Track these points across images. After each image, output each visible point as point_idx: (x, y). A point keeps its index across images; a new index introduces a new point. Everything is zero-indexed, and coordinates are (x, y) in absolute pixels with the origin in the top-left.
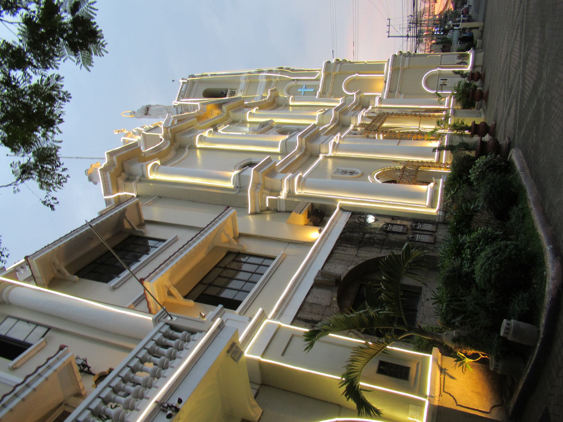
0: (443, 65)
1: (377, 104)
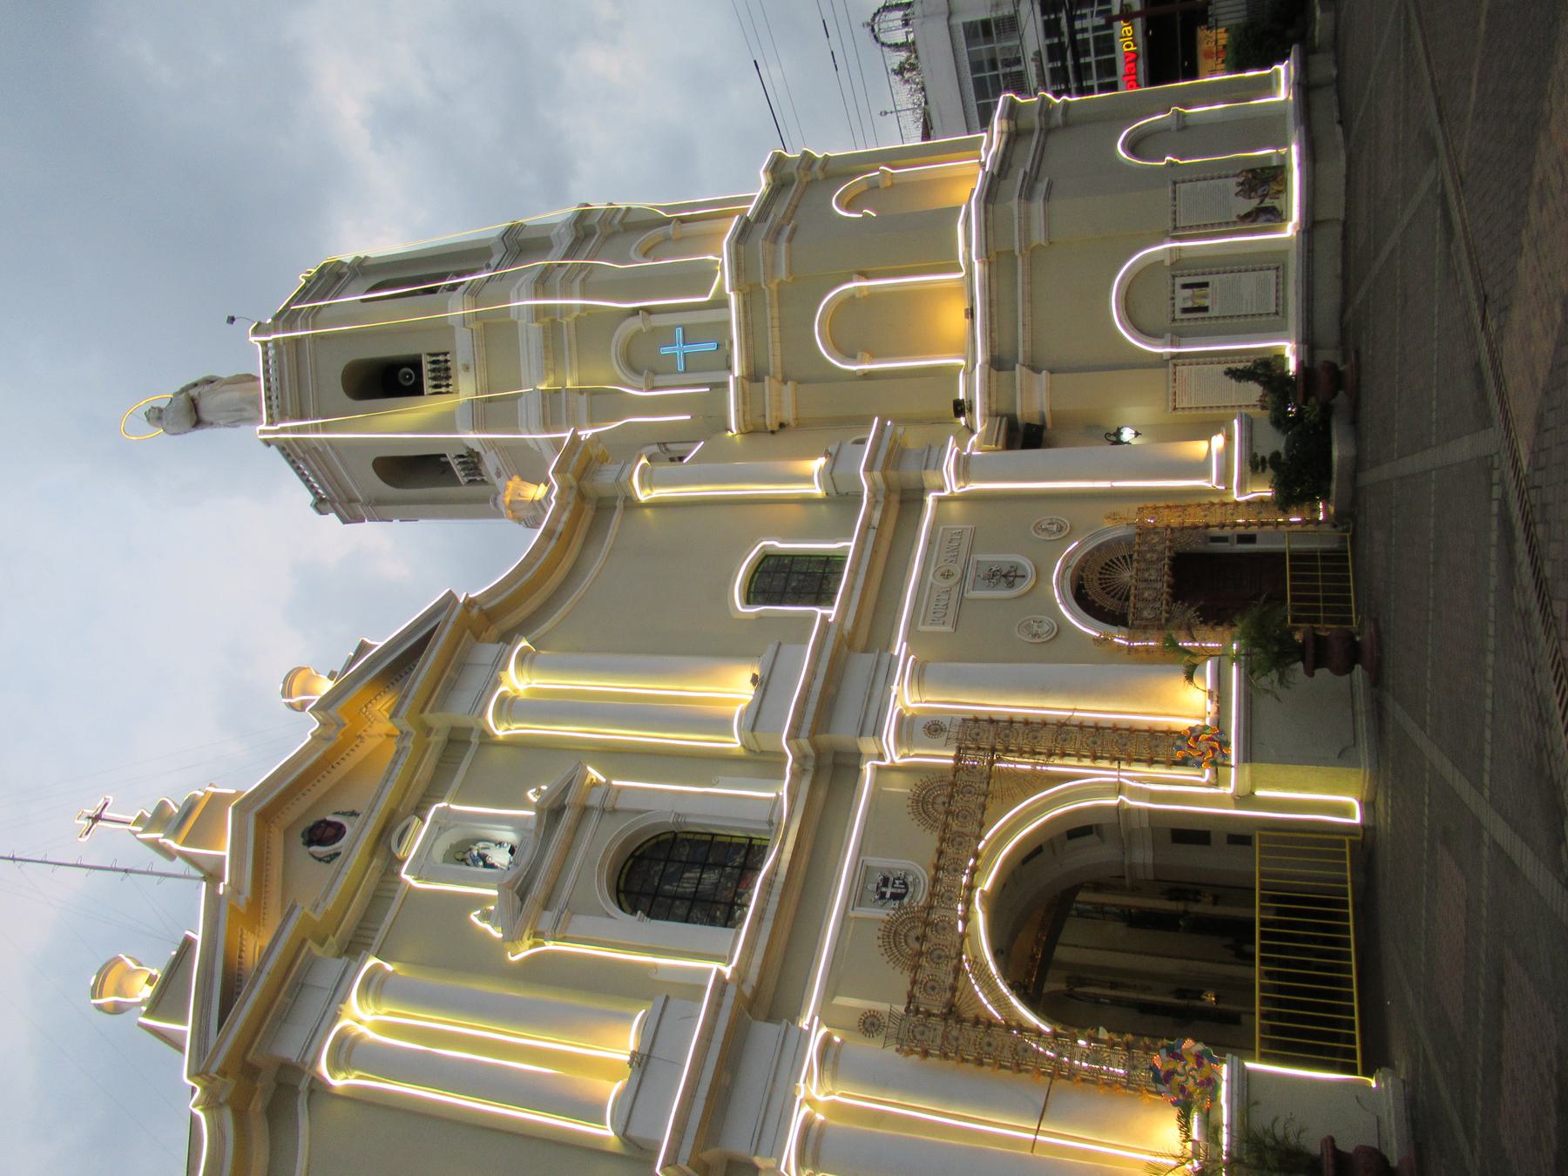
0: (1184, 228)
1: (953, 487)
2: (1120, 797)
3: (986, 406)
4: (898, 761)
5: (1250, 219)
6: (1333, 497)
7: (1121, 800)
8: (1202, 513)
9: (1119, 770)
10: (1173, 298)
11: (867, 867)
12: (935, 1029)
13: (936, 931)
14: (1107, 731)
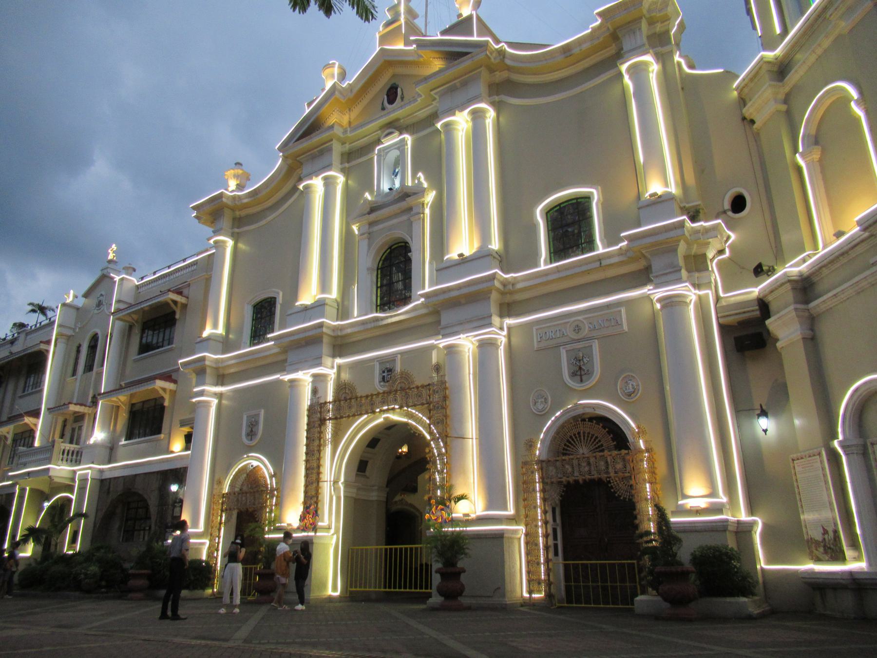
11: (395, 360)
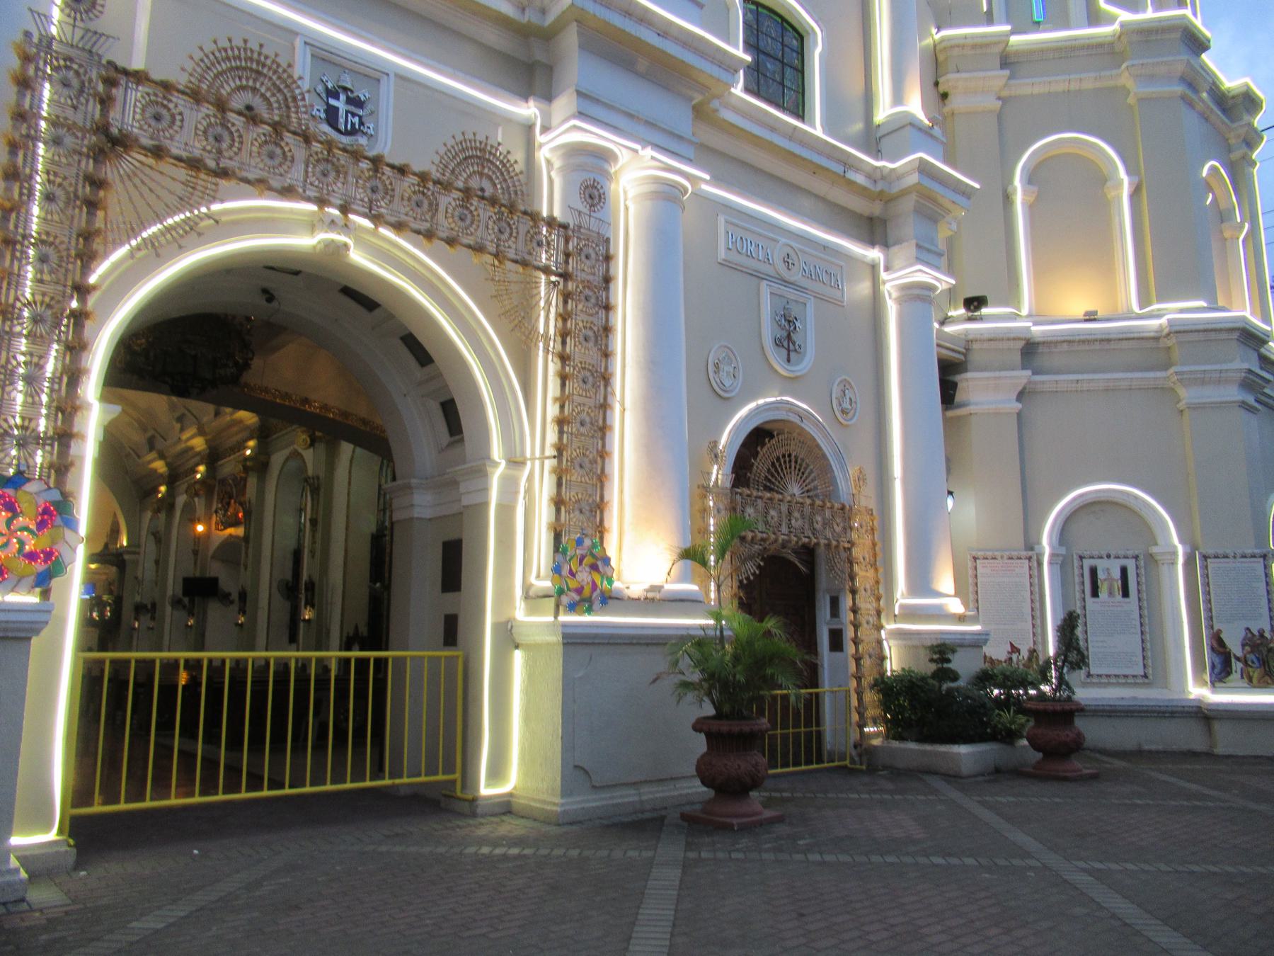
1: (891, 284)
2: (503, 463)
3: (979, 337)
4: (542, 155)
5: (1215, 645)
6: (896, 744)
7: (500, 463)
8: (868, 587)
9: (543, 458)
10: (1109, 556)
12: (75, 108)
13: (266, 142)
14: (600, 443)
